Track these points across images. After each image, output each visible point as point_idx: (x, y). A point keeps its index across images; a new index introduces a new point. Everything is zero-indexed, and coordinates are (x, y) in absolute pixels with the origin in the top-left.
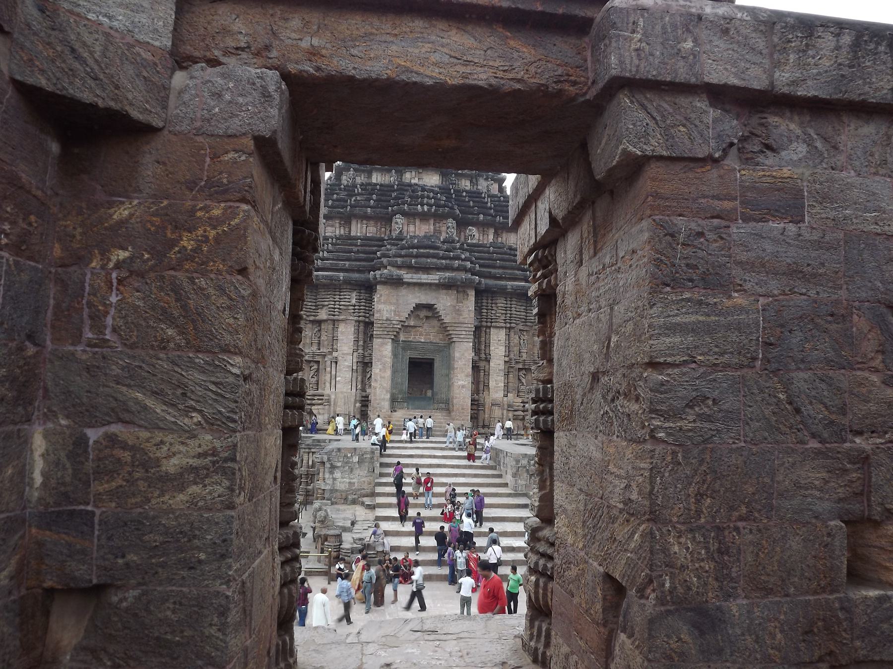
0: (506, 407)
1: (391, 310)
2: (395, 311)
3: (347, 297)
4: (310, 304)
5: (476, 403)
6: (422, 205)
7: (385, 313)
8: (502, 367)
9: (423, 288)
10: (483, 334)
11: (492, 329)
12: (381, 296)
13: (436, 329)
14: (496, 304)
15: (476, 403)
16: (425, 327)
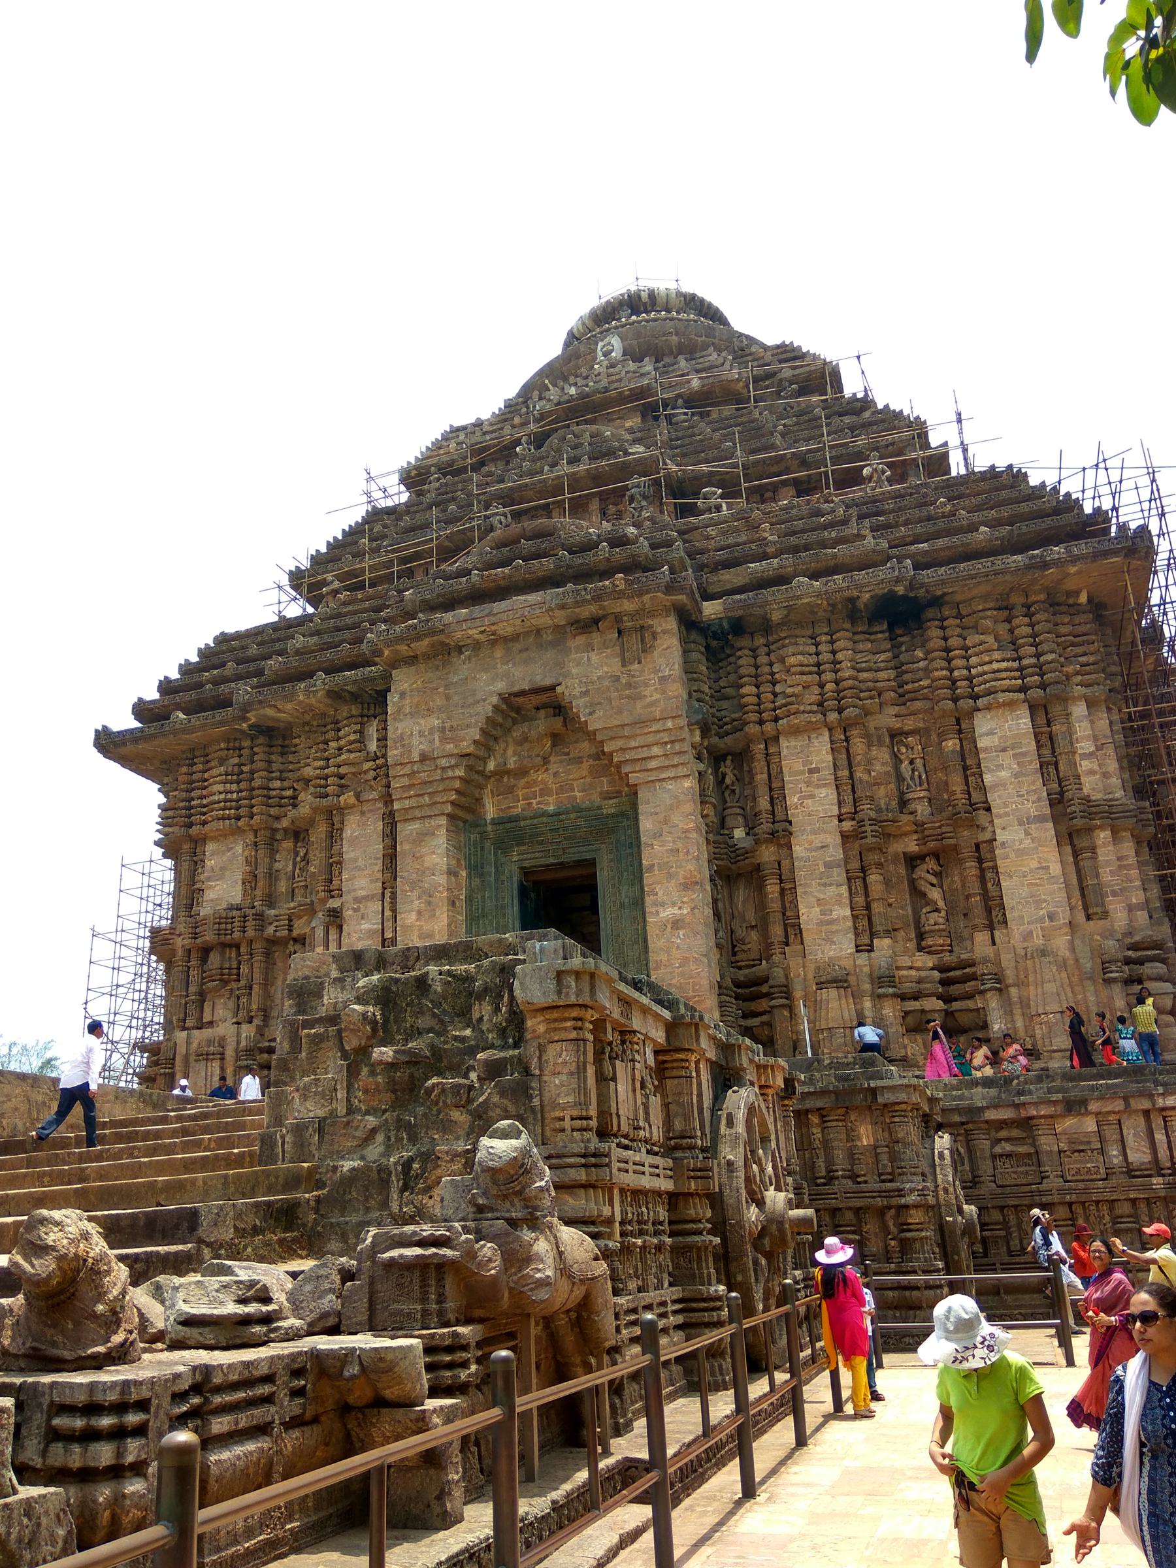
0: (867, 986)
1: (431, 731)
2: (442, 730)
3: (353, 737)
4: (277, 784)
5: (764, 989)
6: (553, 465)
7: (416, 740)
8: (836, 853)
9: (517, 646)
10: (759, 765)
11: (787, 745)
12: (402, 695)
13: (586, 765)
14: (782, 660)
15: (764, 989)
16: (553, 768)
